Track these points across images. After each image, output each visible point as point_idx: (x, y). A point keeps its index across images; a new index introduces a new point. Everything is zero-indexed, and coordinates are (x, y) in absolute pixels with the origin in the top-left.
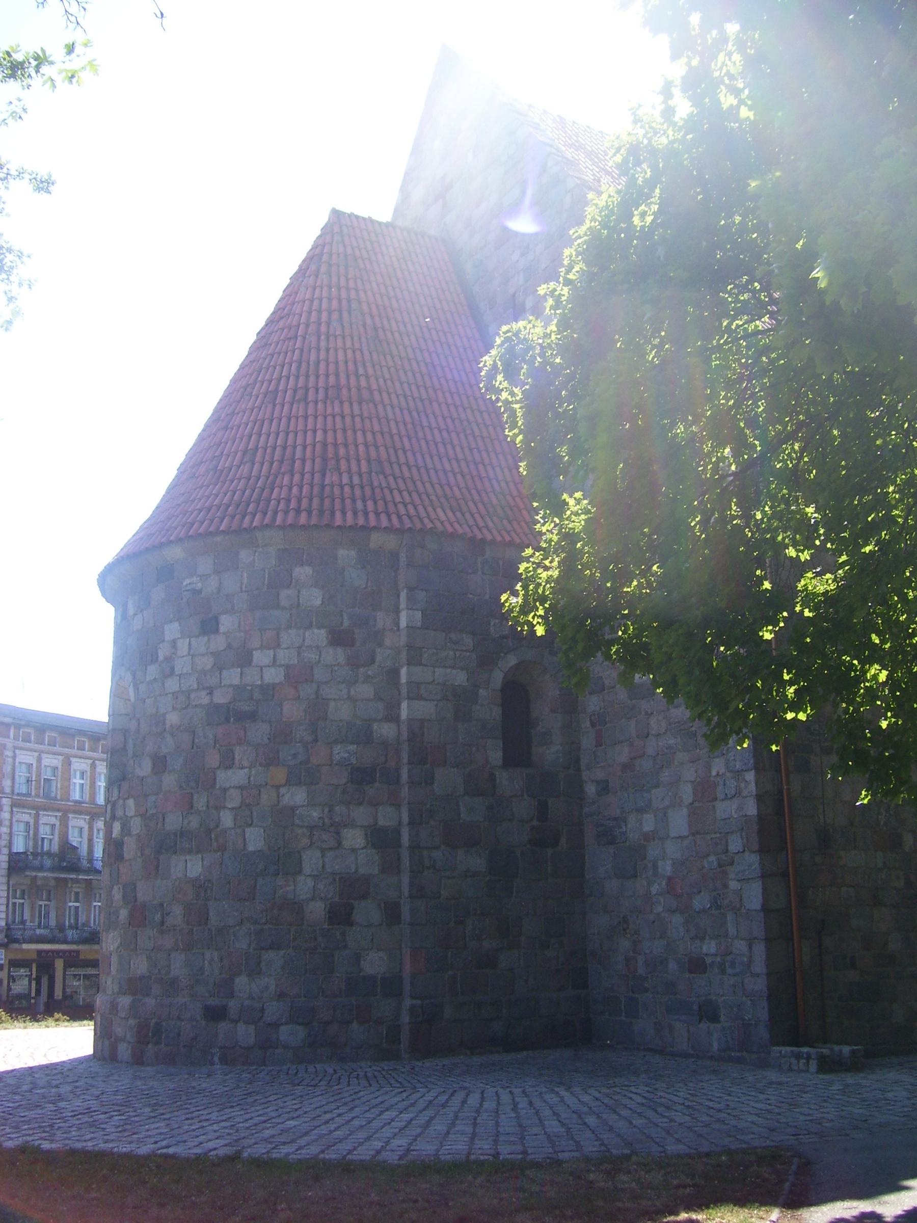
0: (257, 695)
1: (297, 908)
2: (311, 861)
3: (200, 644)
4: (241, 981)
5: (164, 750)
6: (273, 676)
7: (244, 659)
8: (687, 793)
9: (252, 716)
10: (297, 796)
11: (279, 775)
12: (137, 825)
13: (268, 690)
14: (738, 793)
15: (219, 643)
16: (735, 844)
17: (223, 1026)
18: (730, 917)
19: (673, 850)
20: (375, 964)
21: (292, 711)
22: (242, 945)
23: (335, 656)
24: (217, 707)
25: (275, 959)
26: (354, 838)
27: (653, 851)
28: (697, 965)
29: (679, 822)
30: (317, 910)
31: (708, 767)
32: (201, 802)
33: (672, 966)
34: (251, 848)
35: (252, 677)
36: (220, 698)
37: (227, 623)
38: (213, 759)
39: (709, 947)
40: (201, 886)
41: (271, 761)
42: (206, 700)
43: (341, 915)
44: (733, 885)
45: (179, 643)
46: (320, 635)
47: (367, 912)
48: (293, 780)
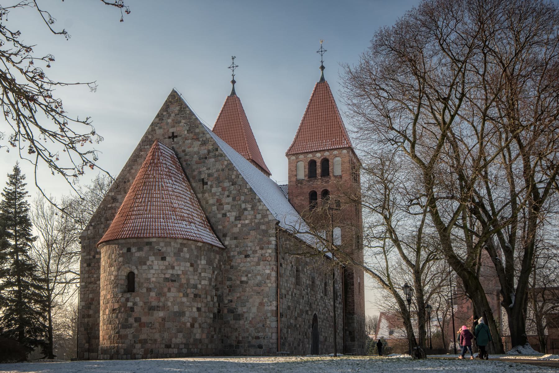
0: (176, 276)
1: (185, 324)
2: (187, 314)
3: (161, 262)
4: (174, 340)
5: (150, 287)
6: (180, 272)
7: (173, 268)
8: (257, 304)
9: (175, 281)
10: (184, 299)
11: (181, 295)
12: (141, 304)
13: (178, 275)
14: (271, 305)
15: (166, 263)
16: (269, 315)
17: (170, 349)
18: (267, 329)
19: (251, 315)
20: (198, 336)
21: (184, 281)
22: (174, 332)
23: (191, 269)
24: (167, 278)
25: (180, 335)
26: (195, 309)
27: (246, 315)
28: (257, 338)
29: (254, 310)
30: (188, 325)
31: (263, 300)
32: (163, 299)
33: (250, 338)
34: (175, 310)
35: (175, 272)
36: (167, 276)
37: (168, 259)
38: (166, 290)
39: (261, 334)
40: (163, 319)
41: (179, 292)
42: (163, 276)
43: (192, 326)
44: (268, 322)
45: (155, 262)
46: (188, 264)
47: (197, 325)
48: (184, 296)
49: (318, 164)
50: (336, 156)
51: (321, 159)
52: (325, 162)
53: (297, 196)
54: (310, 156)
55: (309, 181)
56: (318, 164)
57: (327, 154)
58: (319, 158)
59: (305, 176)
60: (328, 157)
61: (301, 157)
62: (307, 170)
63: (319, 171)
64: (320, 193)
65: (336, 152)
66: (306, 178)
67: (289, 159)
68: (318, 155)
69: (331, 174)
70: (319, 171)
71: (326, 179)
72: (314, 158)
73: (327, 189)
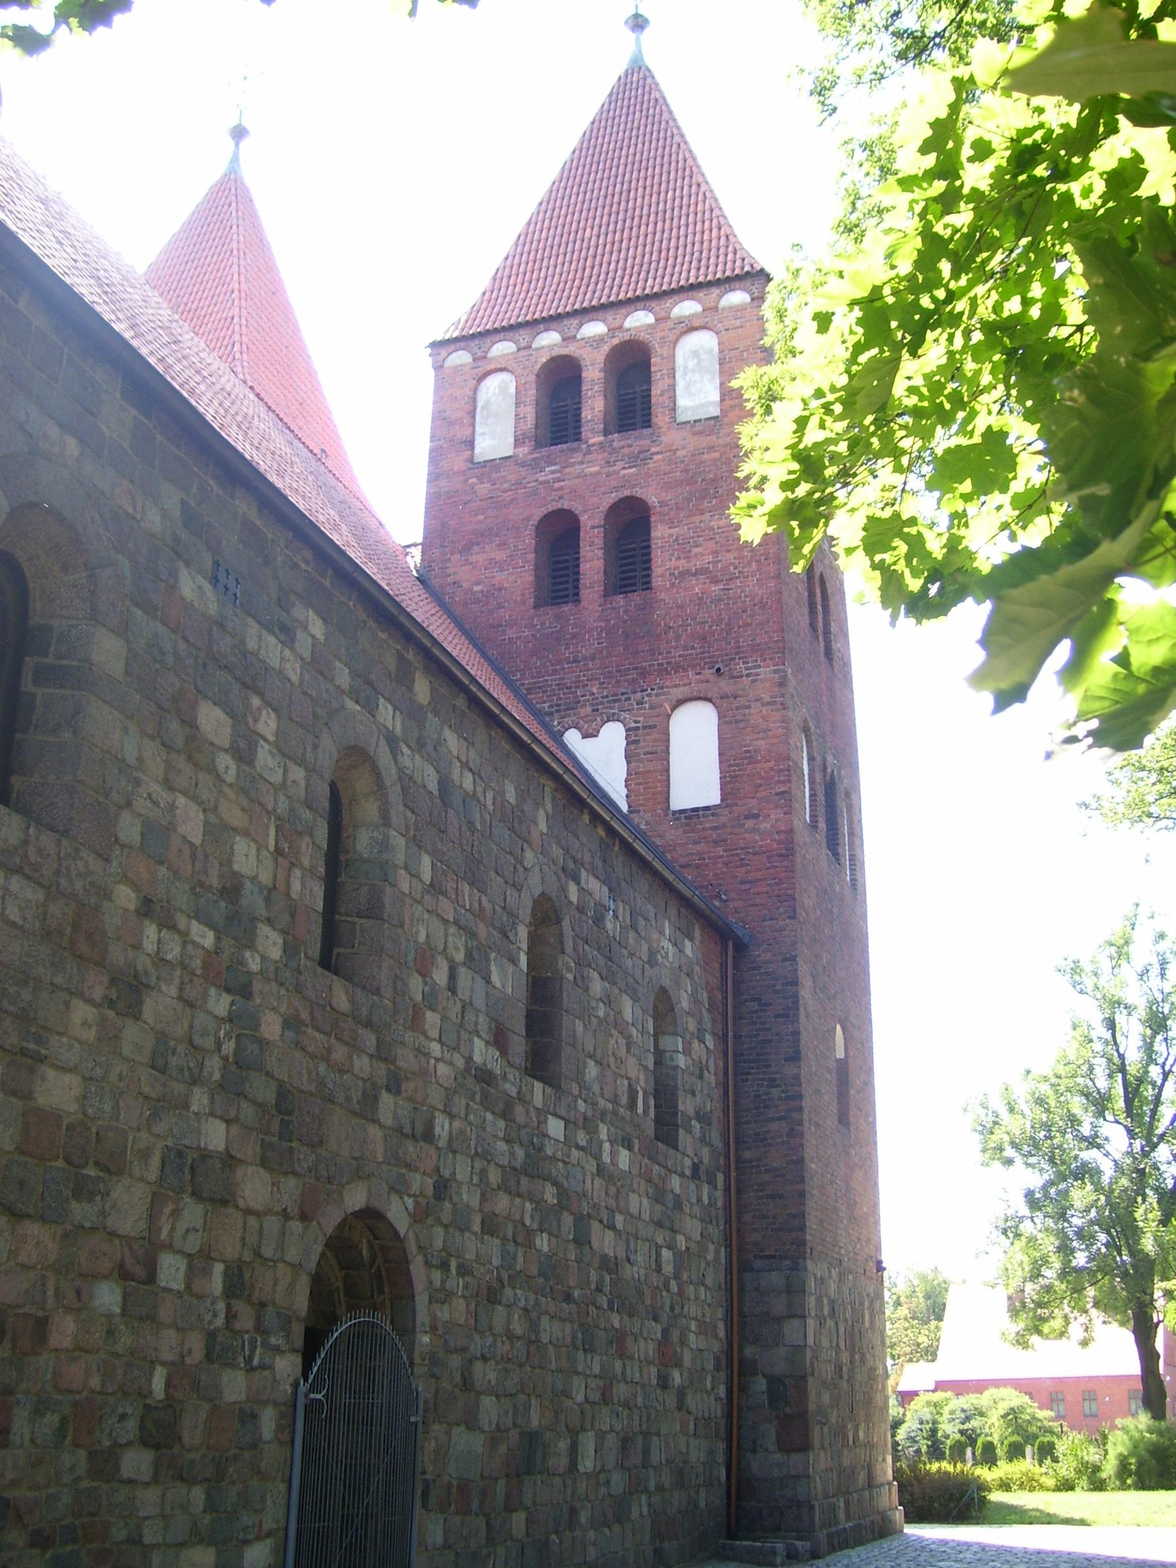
49: (593, 374)
50: (690, 327)
51: (606, 348)
52: (634, 369)
53: (467, 548)
54: (549, 339)
55: (535, 466)
56: (593, 374)
57: (639, 320)
58: (599, 340)
59: (518, 442)
60: (643, 336)
61: (502, 348)
62: (530, 412)
63: (594, 405)
64: (599, 520)
65: (687, 308)
66: (524, 451)
67: (438, 367)
68: (594, 328)
69: (660, 418)
70: (594, 405)
71: (635, 441)
72: (571, 350)
73: (638, 492)
